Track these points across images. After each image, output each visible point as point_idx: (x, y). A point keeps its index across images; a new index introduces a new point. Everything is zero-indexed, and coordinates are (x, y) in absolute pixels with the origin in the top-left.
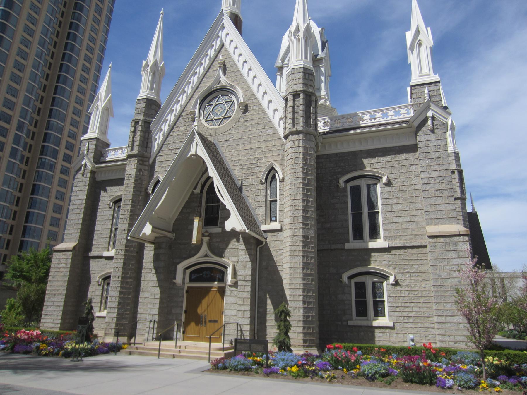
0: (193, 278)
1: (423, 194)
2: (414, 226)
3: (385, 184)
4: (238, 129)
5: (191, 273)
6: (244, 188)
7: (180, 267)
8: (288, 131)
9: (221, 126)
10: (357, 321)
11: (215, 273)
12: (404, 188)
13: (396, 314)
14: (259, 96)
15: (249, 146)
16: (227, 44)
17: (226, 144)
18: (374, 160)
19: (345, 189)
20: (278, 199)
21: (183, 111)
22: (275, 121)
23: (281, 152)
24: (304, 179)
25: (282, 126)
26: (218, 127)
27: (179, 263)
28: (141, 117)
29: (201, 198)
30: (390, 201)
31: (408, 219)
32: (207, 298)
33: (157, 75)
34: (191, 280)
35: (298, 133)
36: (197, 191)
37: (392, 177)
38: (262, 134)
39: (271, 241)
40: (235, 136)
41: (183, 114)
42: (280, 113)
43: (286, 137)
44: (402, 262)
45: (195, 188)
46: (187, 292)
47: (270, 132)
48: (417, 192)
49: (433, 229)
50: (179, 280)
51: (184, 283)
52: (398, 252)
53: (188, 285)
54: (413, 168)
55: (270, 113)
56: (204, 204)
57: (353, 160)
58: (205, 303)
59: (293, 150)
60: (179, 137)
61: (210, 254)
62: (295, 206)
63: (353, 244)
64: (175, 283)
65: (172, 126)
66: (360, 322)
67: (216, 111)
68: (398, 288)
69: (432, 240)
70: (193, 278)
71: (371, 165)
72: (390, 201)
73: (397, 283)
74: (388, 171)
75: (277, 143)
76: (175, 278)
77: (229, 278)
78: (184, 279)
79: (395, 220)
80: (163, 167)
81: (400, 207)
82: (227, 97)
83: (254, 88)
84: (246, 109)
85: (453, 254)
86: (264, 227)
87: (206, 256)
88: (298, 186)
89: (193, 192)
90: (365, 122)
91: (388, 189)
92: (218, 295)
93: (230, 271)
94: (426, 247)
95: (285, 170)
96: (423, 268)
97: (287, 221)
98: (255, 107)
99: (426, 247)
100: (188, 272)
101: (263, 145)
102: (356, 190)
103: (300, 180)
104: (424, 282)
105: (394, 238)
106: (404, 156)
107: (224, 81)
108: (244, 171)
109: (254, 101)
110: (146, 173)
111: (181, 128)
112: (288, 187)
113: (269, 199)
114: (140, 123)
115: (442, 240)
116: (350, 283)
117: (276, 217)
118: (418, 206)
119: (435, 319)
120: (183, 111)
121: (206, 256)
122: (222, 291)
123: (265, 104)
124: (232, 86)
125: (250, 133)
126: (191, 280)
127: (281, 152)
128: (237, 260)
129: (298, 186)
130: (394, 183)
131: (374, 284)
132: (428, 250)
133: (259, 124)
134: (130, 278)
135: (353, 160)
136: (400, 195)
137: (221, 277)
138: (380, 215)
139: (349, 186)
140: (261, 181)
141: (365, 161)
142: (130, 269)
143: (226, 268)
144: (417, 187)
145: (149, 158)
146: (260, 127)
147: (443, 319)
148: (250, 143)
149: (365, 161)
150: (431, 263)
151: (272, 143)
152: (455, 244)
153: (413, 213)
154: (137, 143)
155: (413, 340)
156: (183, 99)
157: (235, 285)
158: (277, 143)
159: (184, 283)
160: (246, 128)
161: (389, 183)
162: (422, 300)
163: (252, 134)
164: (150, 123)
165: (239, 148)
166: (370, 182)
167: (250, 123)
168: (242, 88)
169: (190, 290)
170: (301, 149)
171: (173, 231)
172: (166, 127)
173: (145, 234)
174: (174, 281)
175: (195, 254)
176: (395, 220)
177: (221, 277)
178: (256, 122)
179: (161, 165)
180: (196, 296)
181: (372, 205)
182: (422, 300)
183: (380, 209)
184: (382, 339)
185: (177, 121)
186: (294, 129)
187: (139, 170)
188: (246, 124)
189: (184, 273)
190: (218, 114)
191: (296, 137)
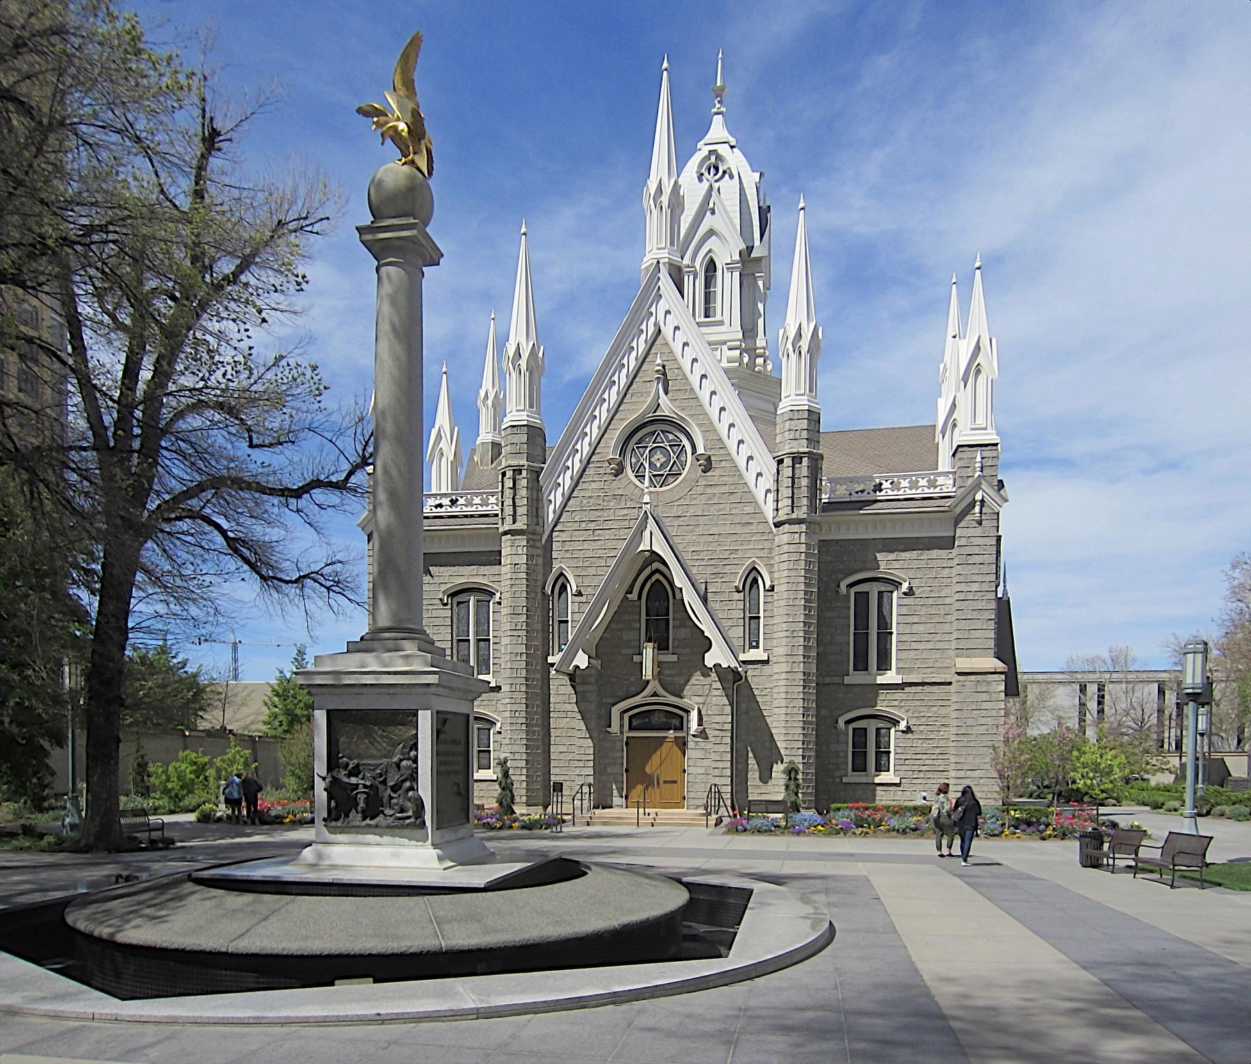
1: (956, 615)
2: (938, 655)
3: (905, 593)
5: (631, 718)
6: (709, 596)
7: (615, 711)
8: (782, 516)
9: (664, 488)
10: (853, 777)
11: (676, 719)
12: (930, 601)
13: (904, 768)
14: (732, 445)
17: (676, 523)
18: (892, 556)
19: (848, 595)
20: (761, 614)
21: (593, 453)
22: (759, 494)
23: (767, 545)
24: (806, 593)
25: (771, 505)
26: (658, 489)
28: (524, 462)
30: (910, 619)
31: (930, 646)
32: (658, 753)
33: (535, 373)
35: (799, 521)
36: (634, 596)
37: (915, 584)
38: (736, 511)
39: (754, 677)
40: (692, 511)
41: (594, 458)
42: (767, 482)
43: (777, 525)
44: (919, 703)
45: (630, 591)
47: (749, 509)
48: (947, 608)
49: (964, 664)
50: (615, 728)
51: (622, 732)
52: (913, 689)
54: (946, 572)
55: (750, 478)
57: (863, 552)
58: (656, 758)
59: (792, 548)
60: (592, 500)
61: (661, 691)
63: (854, 678)
65: (576, 478)
66: (859, 778)
68: (909, 736)
69: (961, 678)
71: (888, 563)
72: (910, 619)
73: (908, 730)
74: (911, 574)
75: (761, 528)
77: (694, 725)
78: (622, 726)
79: (914, 646)
81: (921, 628)
82: (671, 437)
83: (723, 429)
84: (708, 465)
85: (984, 697)
86: (742, 657)
87: (655, 694)
88: (797, 602)
89: (625, 598)
90: (883, 493)
91: (908, 601)
92: (676, 749)
93: (694, 715)
94: (950, 683)
95: (776, 575)
96: (943, 711)
97: (780, 651)
99: (950, 683)
100: (626, 716)
101: (738, 529)
102: (863, 598)
103: (802, 595)
104: (943, 729)
105: (910, 670)
106: (935, 553)
107: (667, 407)
108: (709, 570)
109: (722, 452)
110: (540, 561)
111: (593, 485)
112: (783, 603)
113: (748, 615)
114: (524, 473)
115: (972, 678)
116: (847, 729)
117: (758, 643)
118: (947, 628)
119: (953, 774)
120: (593, 453)
122: (682, 744)
123: (741, 462)
125: (717, 507)
126: (630, 729)
127: (767, 545)
128: (705, 703)
129: (797, 602)
130: (917, 592)
131: (878, 730)
132: (952, 688)
134: (536, 725)
135: (863, 552)
136: (923, 611)
138: (894, 636)
139: (853, 591)
140: (737, 587)
141: (879, 556)
142: (536, 713)
143: (687, 712)
144: (947, 601)
146: (733, 499)
147: (962, 774)
148: (716, 525)
149: (879, 556)
150: (955, 706)
151: (754, 528)
152: (989, 683)
153: (938, 637)
154: (522, 510)
155: (924, 798)
156: (594, 430)
157: (703, 734)
158: (761, 528)
159: (622, 732)
161: (910, 592)
162: (938, 751)
163: (720, 510)
164: (538, 473)
165: (700, 530)
166: (883, 587)
167: (716, 490)
168: (699, 425)
170: (803, 548)
171: (597, 657)
172: (566, 480)
173: (577, 667)
176: (914, 646)
178: (726, 489)
180: (639, 752)
181: (884, 624)
182: (938, 751)
183: (894, 630)
184: (883, 798)
185: (584, 471)
186: (794, 516)
187: (530, 557)
188: (709, 490)
189: (622, 718)
191: (795, 528)
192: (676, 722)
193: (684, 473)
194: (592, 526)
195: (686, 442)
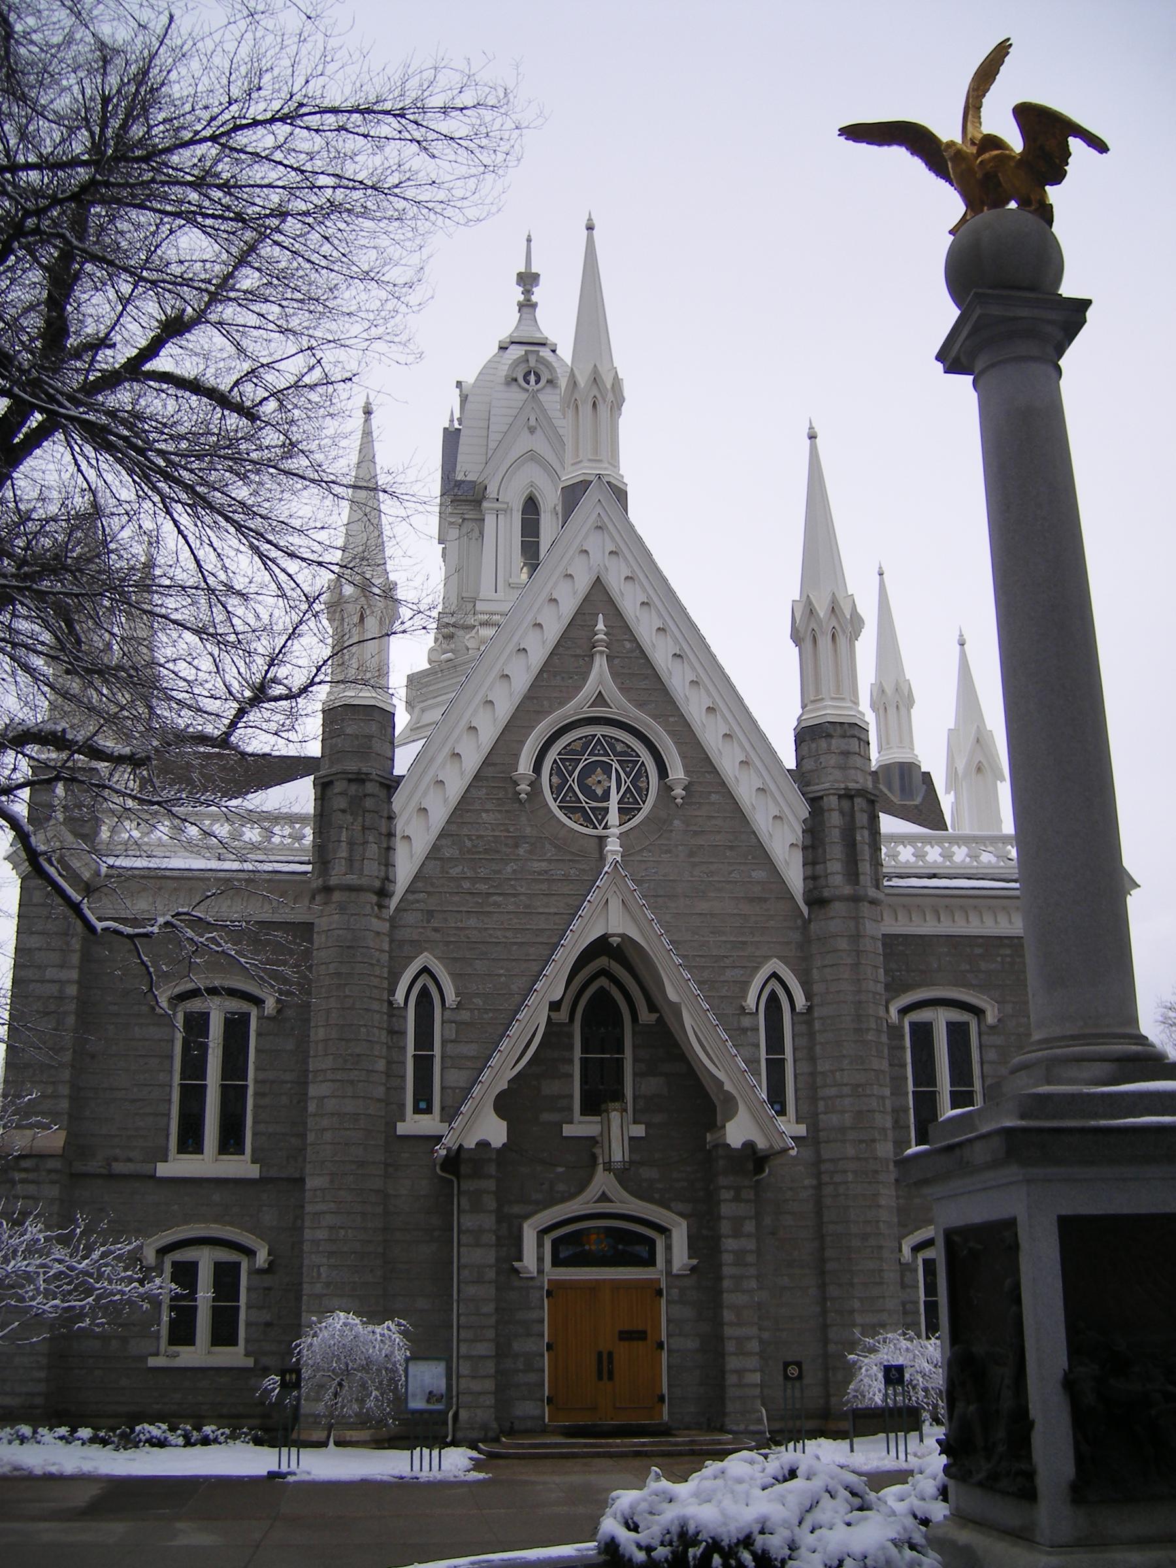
0: (562, 1256)
4: (667, 852)
5: (555, 1243)
15: (703, 906)
16: (615, 583)
27: (527, 1217)
29: (571, 1036)
34: (556, 1262)
36: (563, 1016)
46: (549, 1294)
47: (759, 875)
50: (529, 1261)
53: (553, 1274)
56: (577, 1054)
62: (858, 1086)
64: (516, 1271)
67: (589, 781)
70: (562, 1256)
76: (520, 1259)
78: (540, 1259)
80: (436, 930)
98: (714, 797)
121: (604, 1198)
124: (636, 719)
126: (556, 1262)
133: (731, 848)
137: (645, 1255)
145: (389, 895)
159: (541, 1271)
160: (691, 854)
169: (555, 1291)
174: (516, 1264)
175: (572, 1196)
177: (645, 1255)
179: (428, 922)
189: (540, 1245)
190: (599, 792)
192: (643, 1251)
193: (647, 808)
194: (483, 887)
195: (646, 757)
